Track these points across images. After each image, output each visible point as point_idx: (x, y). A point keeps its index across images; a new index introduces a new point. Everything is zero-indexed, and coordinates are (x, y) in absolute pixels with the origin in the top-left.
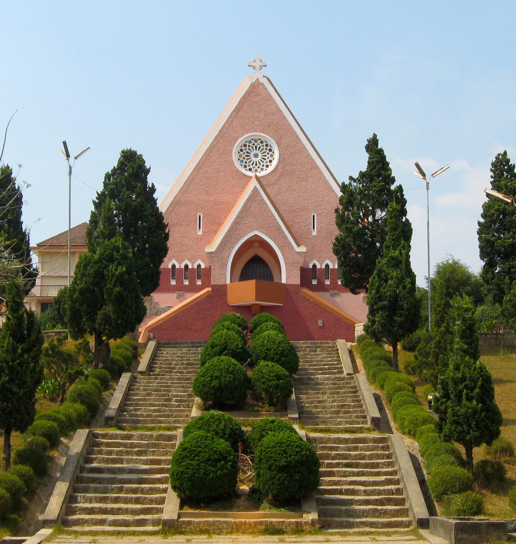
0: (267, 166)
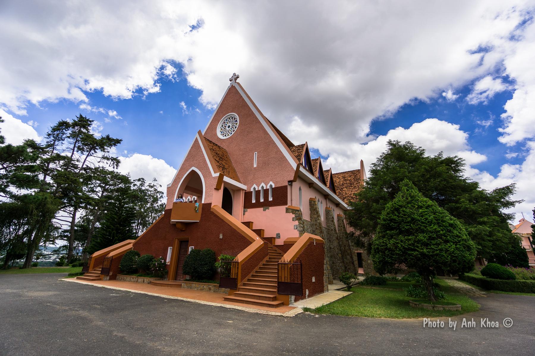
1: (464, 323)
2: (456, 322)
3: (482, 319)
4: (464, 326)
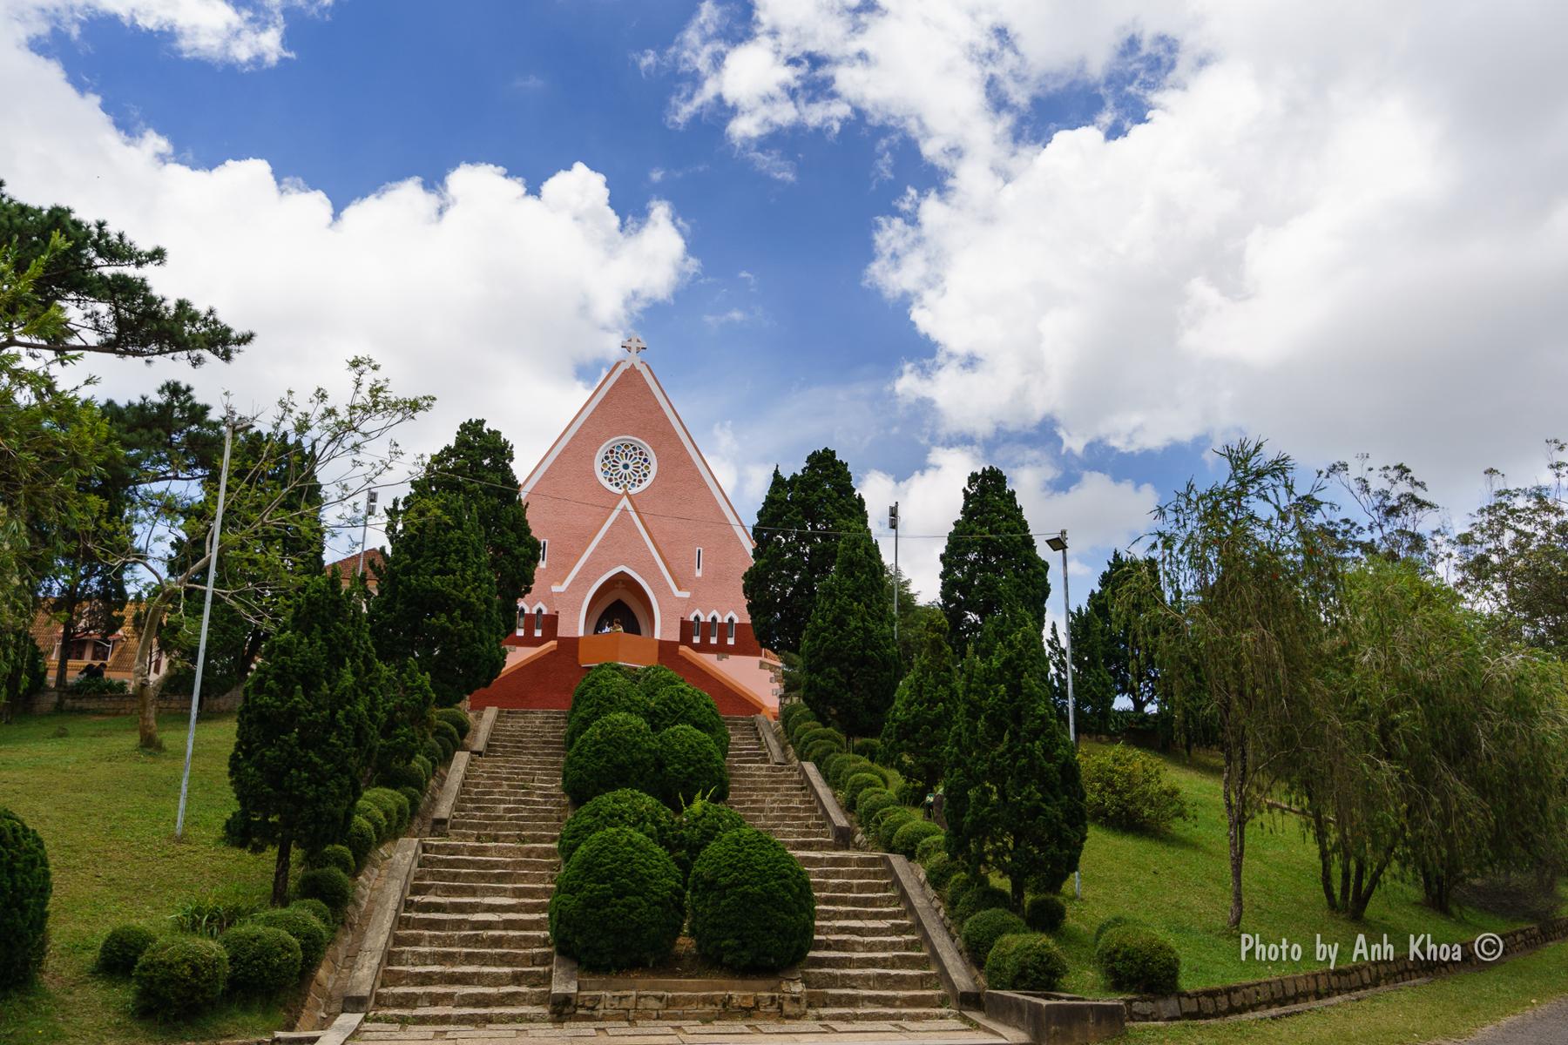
0: (640, 481)
1: (1361, 947)
2: (1337, 945)
3: (1412, 937)
4: (1360, 956)
